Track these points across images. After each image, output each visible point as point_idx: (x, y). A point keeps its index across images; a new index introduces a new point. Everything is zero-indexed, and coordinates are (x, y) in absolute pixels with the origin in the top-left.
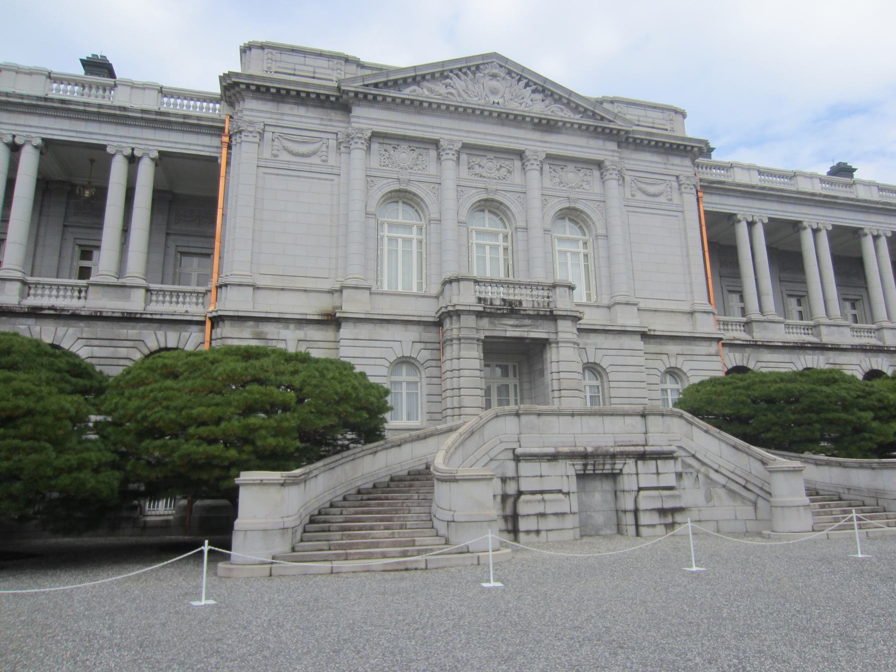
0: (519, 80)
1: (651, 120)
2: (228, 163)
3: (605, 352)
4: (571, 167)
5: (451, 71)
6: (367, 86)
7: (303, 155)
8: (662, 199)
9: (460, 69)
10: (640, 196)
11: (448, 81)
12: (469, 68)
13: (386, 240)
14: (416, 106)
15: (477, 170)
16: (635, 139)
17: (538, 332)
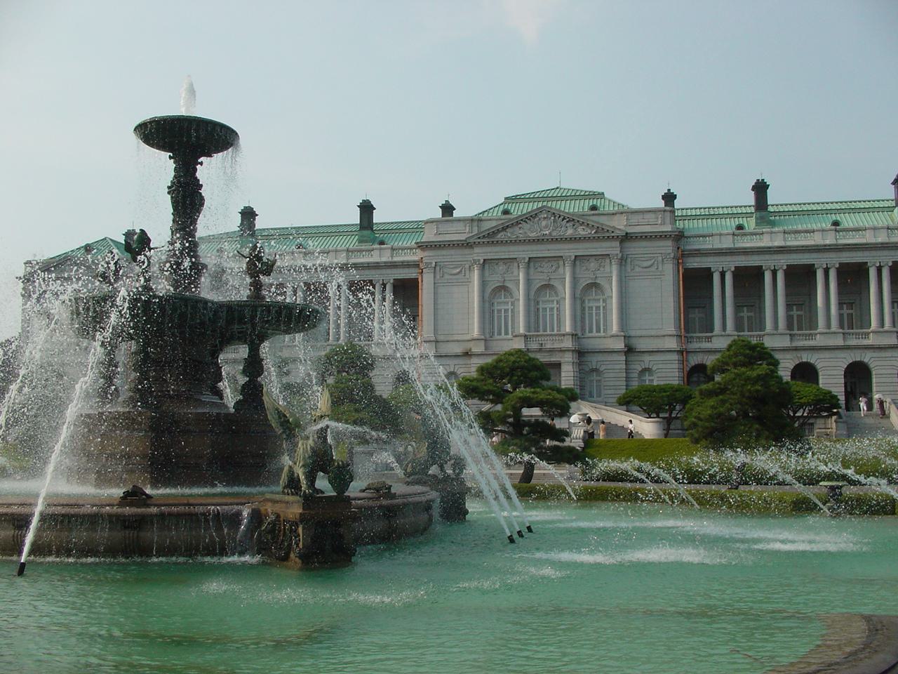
0: (560, 217)
1: (646, 220)
2: (422, 281)
3: (602, 363)
4: (592, 259)
5: (522, 220)
6: (479, 238)
7: (454, 275)
8: (653, 269)
9: (527, 218)
10: (637, 269)
11: (520, 225)
12: (531, 216)
13: (496, 311)
14: (501, 243)
15: (540, 269)
16: (632, 237)
17: (554, 359)
